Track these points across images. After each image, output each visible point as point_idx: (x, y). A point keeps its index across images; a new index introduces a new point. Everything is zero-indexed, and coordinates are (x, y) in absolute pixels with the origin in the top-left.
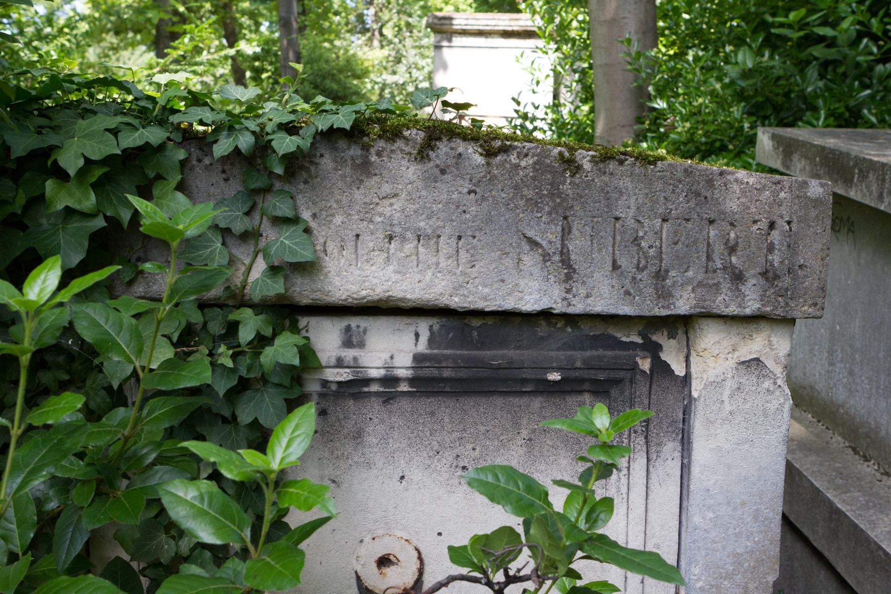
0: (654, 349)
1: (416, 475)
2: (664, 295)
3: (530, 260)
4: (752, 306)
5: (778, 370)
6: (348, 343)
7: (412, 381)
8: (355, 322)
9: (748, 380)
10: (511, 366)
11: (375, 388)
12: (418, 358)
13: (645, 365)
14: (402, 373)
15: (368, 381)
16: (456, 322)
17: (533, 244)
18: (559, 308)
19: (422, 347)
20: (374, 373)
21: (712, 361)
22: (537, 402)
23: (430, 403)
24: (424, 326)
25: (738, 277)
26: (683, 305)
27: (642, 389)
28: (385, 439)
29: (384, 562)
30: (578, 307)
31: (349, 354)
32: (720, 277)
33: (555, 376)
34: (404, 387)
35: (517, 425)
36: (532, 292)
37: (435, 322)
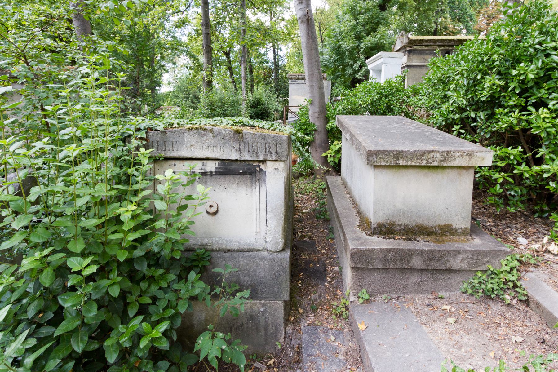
0: (259, 166)
1: (216, 190)
2: (258, 156)
3: (234, 150)
4: (274, 158)
5: (281, 170)
6: (203, 165)
7: (215, 172)
8: (204, 161)
9: (276, 172)
10: (233, 169)
11: (209, 174)
12: (216, 168)
13: (258, 169)
14: (213, 171)
15: (207, 172)
16: (223, 161)
17: (234, 148)
18: (239, 159)
19: (217, 166)
20: (208, 171)
21: (269, 168)
22: (239, 176)
23: (220, 176)
24: (217, 162)
25: (271, 153)
26: (261, 158)
27: (258, 174)
28: (211, 183)
29: (211, 206)
30: (242, 159)
31: (203, 167)
32: (268, 153)
33: (241, 171)
34: (214, 173)
35: (235, 180)
36: (234, 156)
37: (219, 161)
